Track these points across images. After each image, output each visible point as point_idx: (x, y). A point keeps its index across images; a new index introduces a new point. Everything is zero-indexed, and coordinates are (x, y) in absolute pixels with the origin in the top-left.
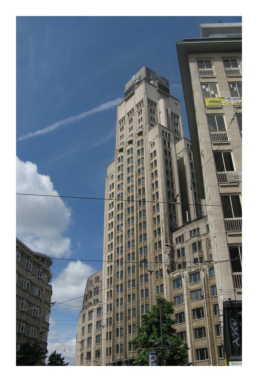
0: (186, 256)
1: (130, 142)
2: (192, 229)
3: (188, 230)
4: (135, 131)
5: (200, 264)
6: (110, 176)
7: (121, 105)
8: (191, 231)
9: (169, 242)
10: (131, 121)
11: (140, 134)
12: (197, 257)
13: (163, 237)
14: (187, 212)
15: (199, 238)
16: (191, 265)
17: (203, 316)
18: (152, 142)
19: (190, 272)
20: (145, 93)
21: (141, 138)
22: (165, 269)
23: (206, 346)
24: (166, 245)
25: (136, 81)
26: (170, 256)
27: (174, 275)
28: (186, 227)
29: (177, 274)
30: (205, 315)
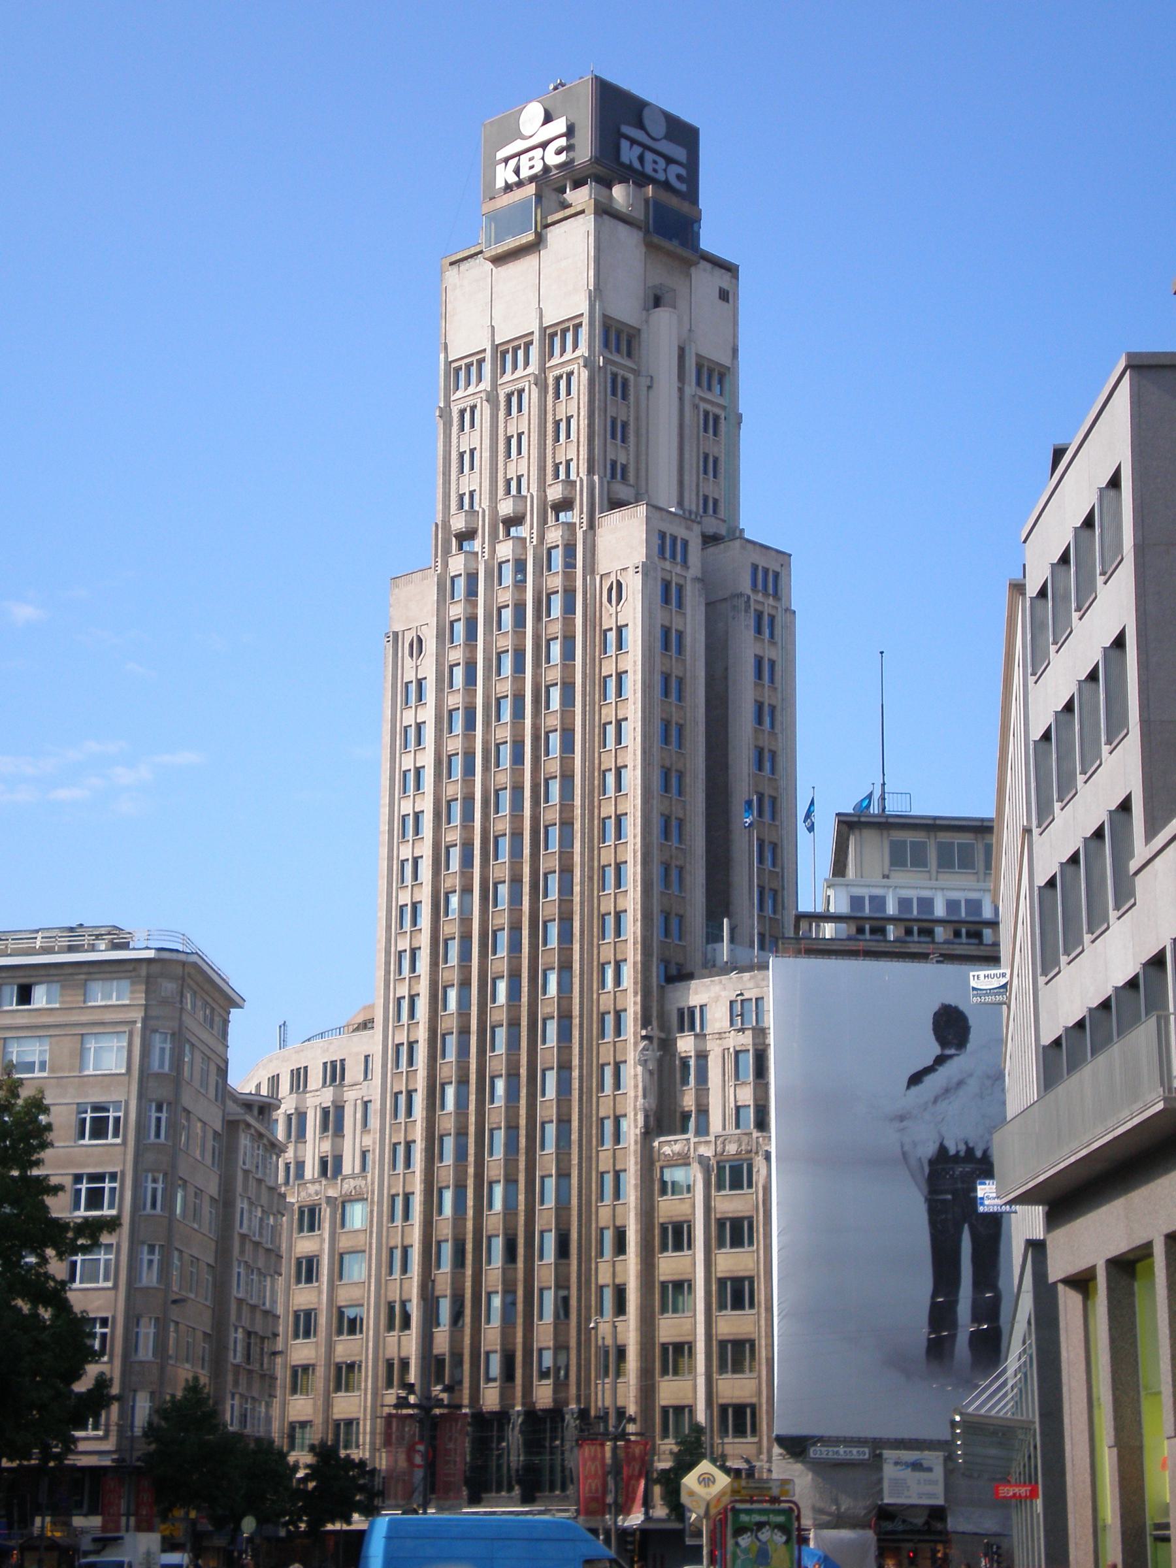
0: (710, 1085)
3: (723, 994)
5: (755, 1134)
7: (464, 266)
9: (655, 1023)
12: (747, 1103)
13: (635, 1003)
14: (725, 920)
15: (761, 1036)
16: (724, 1128)
17: (752, 1305)
18: (613, 578)
19: (722, 1154)
20: (592, 288)
22: (636, 1120)
23: (754, 1400)
24: (644, 1038)
25: (544, 145)
26: (656, 1077)
27: (667, 1150)
28: (721, 982)
29: (677, 1148)
30: (759, 1302)
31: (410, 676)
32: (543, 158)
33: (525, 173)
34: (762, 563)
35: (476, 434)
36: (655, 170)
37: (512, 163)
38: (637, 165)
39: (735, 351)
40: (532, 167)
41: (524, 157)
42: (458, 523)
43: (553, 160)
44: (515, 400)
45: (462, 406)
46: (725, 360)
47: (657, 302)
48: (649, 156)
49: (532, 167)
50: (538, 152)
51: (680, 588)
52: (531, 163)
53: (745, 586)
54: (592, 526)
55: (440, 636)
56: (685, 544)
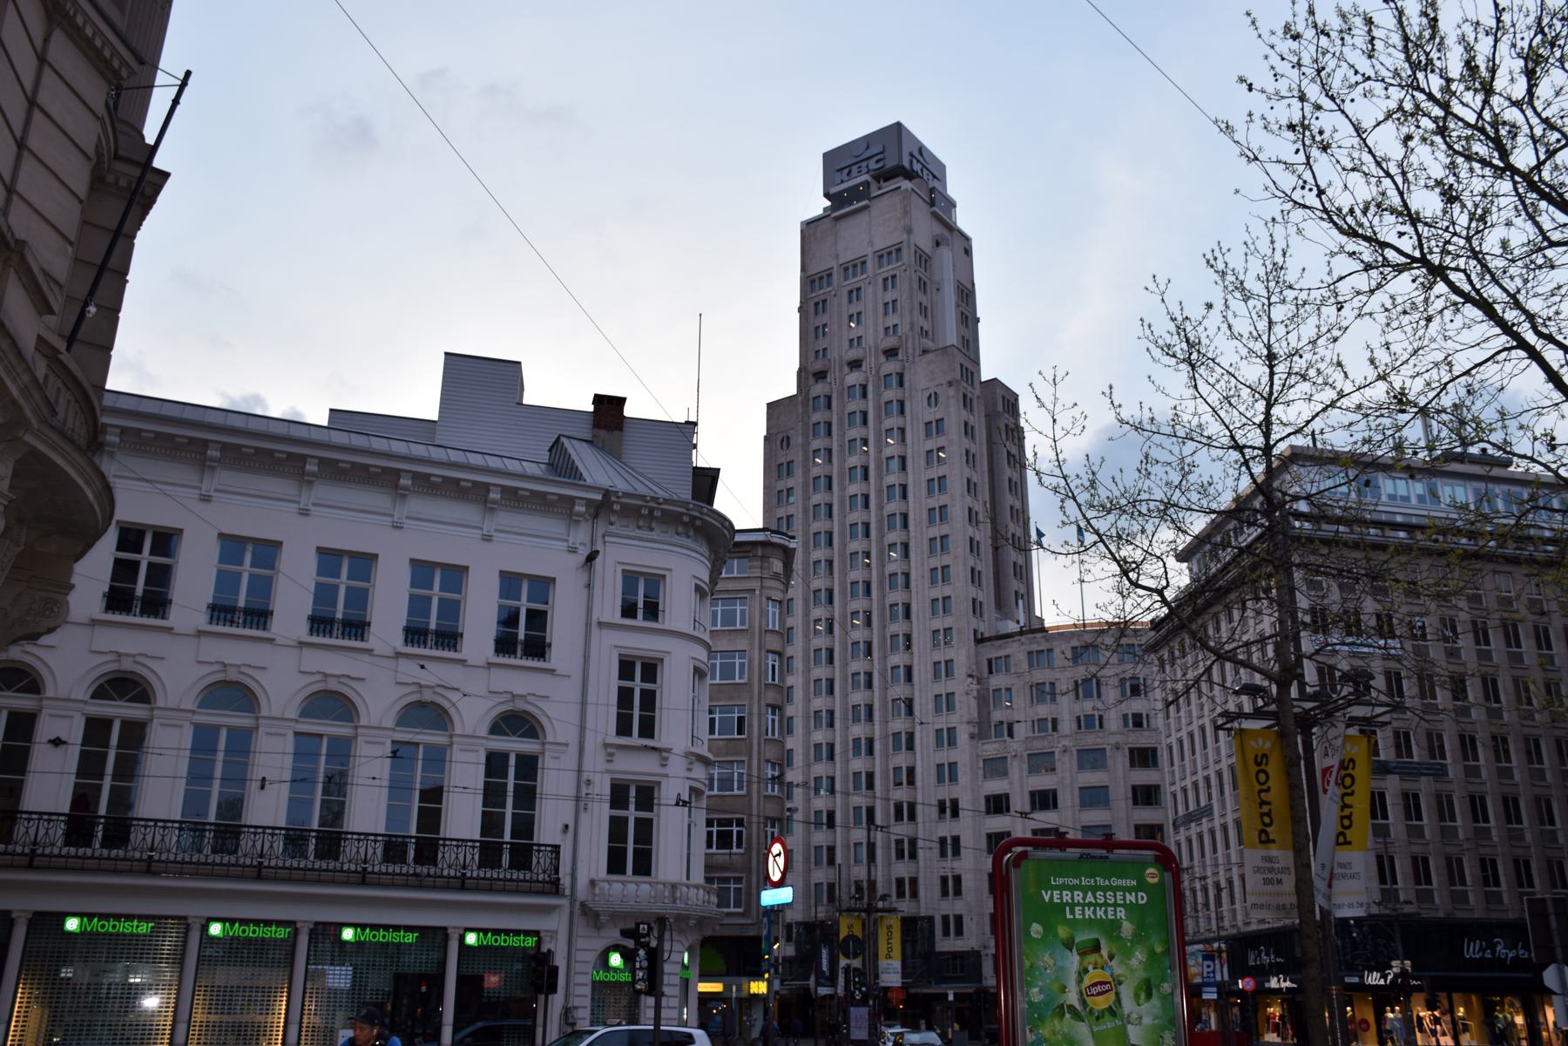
1: (855, 364)
2: (1035, 647)
4: (872, 333)
6: (780, 437)
8: (1030, 653)
10: (855, 294)
11: (891, 353)
18: (932, 391)
21: (891, 367)
24: (970, 676)
31: (783, 460)
34: (1007, 396)
39: (973, 285)
42: (818, 366)
45: (816, 300)
46: (970, 287)
47: (938, 244)
53: (1000, 408)
54: (914, 362)
55: (805, 436)
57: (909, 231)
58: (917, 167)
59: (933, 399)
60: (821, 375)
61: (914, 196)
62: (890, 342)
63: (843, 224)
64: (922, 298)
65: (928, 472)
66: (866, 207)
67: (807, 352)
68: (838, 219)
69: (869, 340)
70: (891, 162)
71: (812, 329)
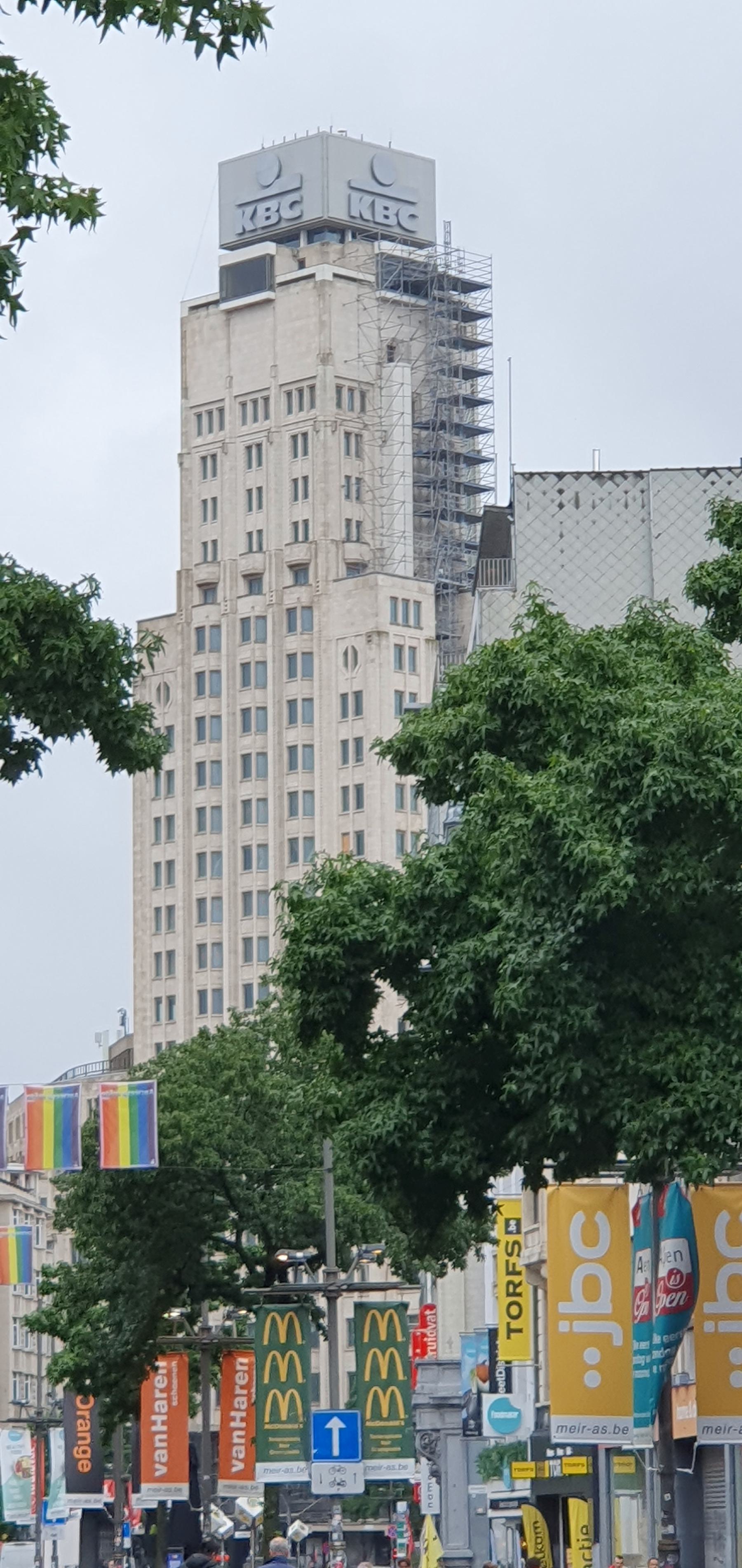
32: (278, 211)
33: (261, 222)
35: (216, 482)
36: (386, 217)
37: (249, 210)
38: (367, 215)
40: (268, 218)
41: (261, 207)
43: (287, 213)
44: (254, 451)
45: (203, 454)
48: (380, 203)
49: (268, 218)
50: (273, 204)
51: (413, 649)
52: (268, 214)
56: (418, 604)
57: (325, 358)
58: (361, 206)
59: (351, 658)
60: (208, 589)
61: (340, 283)
62: (299, 553)
63: (240, 323)
64: (351, 467)
65: (342, 774)
66: (269, 301)
67: (190, 542)
68: (230, 312)
69: (271, 543)
70: (311, 213)
71: (197, 504)
